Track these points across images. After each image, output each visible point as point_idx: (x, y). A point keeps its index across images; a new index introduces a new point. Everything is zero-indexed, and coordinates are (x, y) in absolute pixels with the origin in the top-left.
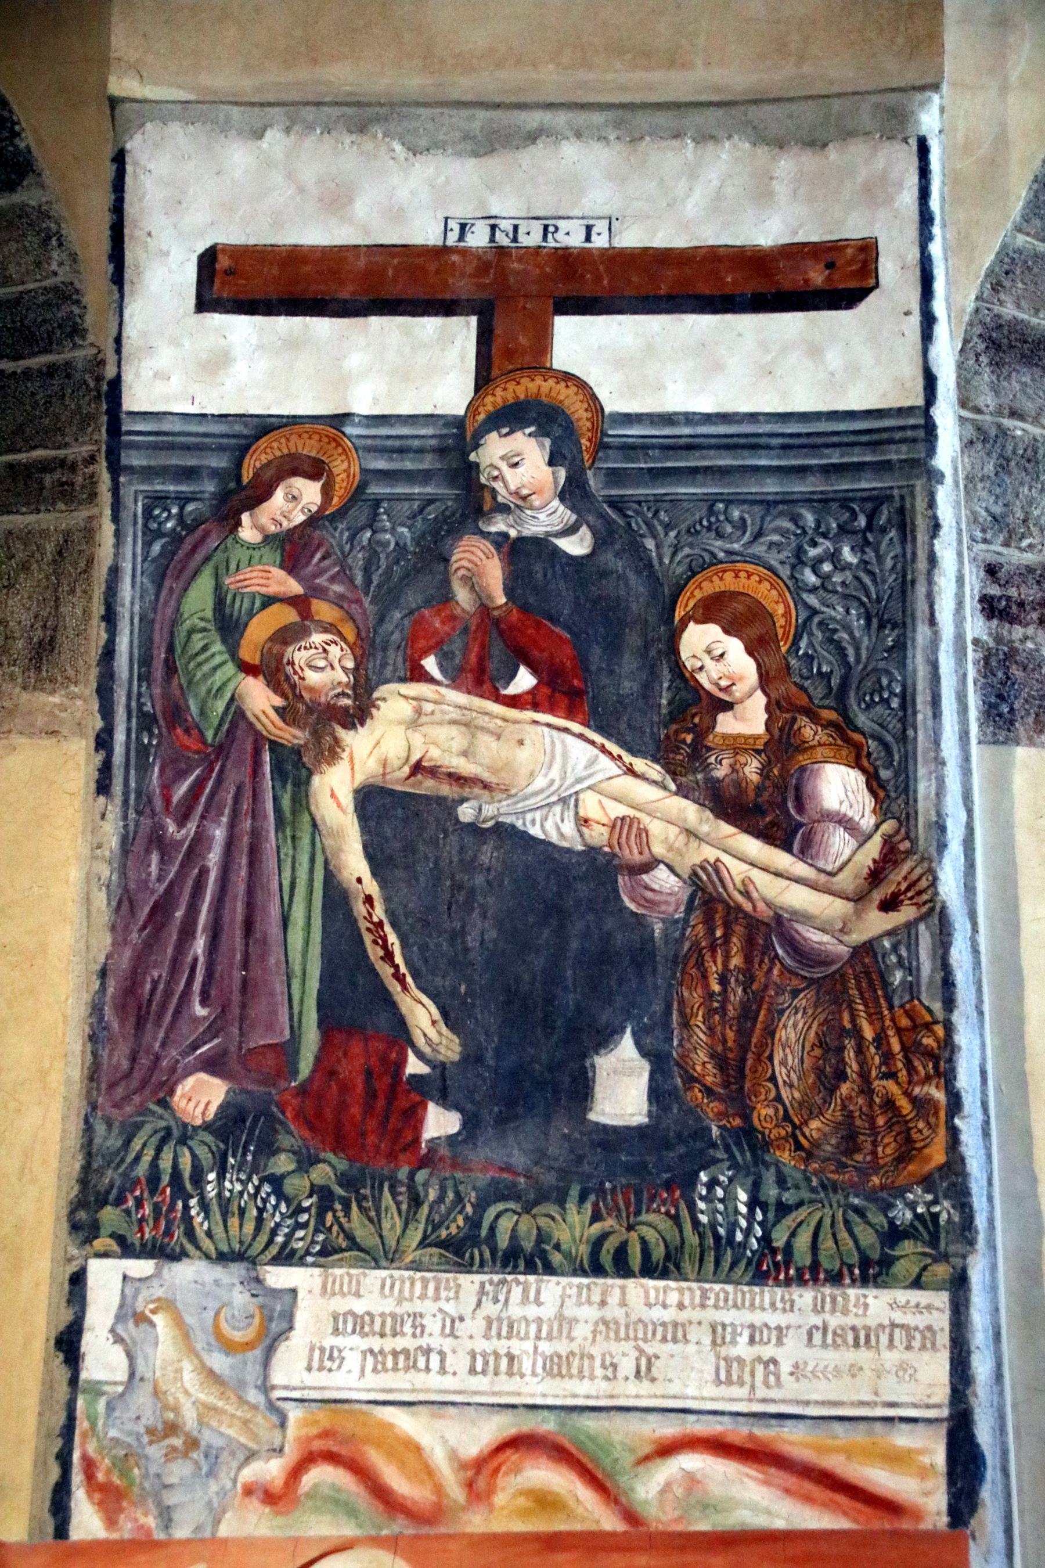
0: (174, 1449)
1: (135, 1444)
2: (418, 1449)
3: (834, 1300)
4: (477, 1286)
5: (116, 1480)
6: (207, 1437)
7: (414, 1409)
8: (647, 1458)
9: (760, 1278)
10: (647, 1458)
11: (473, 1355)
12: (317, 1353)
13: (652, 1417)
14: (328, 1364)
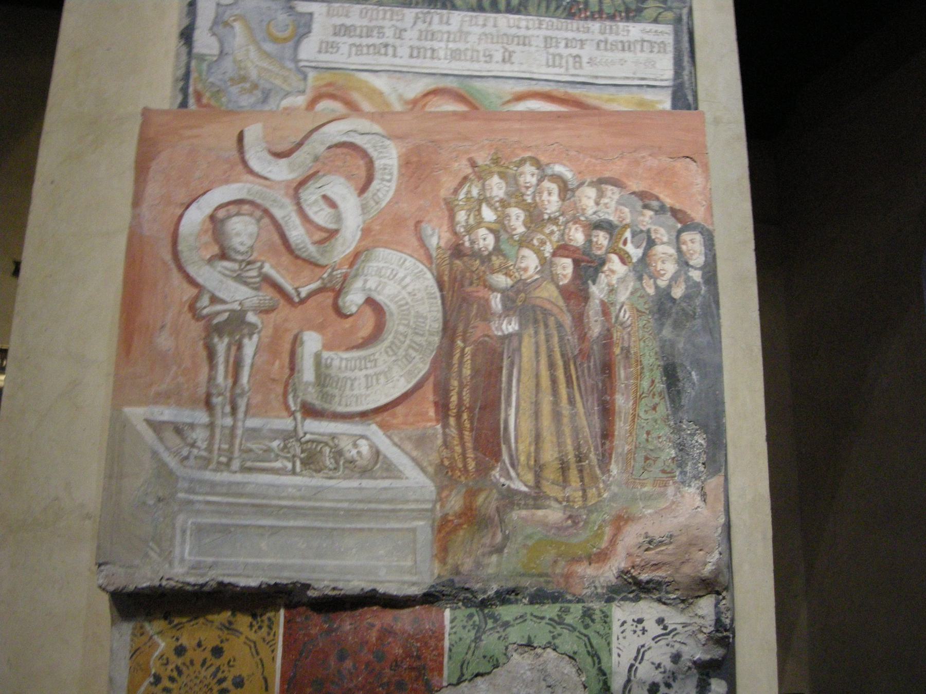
2: (381, 94)
3: (611, 27)
4: (413, 15)
5: (213, 102)
7: (379, 74)
8: (509, 102)
9: (571, 15)
10: (509, 102)
11: (412, 48)
12: (324, 45)
13: (511, 81)
14: (330, 50)
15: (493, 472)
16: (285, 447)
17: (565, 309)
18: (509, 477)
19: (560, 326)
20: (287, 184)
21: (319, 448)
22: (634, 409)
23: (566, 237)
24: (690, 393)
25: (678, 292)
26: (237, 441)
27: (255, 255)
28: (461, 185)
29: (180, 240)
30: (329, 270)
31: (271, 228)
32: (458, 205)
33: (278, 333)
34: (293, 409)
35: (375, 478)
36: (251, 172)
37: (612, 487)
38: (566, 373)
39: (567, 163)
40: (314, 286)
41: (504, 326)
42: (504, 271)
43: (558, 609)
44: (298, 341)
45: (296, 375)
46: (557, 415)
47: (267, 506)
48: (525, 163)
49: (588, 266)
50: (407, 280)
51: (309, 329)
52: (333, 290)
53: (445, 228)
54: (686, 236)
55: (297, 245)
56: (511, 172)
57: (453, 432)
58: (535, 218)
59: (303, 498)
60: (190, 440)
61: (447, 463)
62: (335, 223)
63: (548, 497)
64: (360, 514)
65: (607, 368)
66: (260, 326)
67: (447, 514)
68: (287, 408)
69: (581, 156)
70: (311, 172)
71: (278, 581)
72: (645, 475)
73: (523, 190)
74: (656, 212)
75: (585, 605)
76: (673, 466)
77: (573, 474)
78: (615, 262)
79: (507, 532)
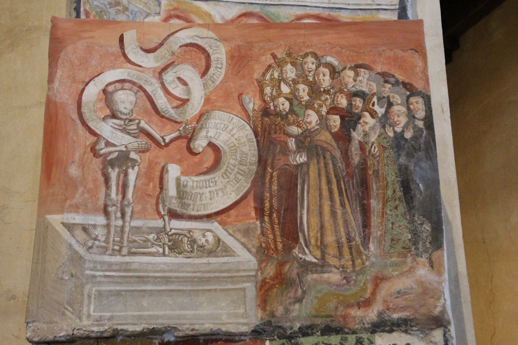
0: (119, 10)
1: (104, 8)
2: (210, 15)
6: (131, 7)
15: (294, 251)
16: (158, 238)
17: (336, 147)
18: (304, 253)
19: (333, 158)
20: (154, 70)
21: (180, 239)
22: (383, 209)
23: (335, 102)
24: (419, 198)
25: (408, 135)
26: (126, 236)
27: (134, 115)
28: (267, 70)
29: (83, 104)
30: (184, 125)
31: (145, 97)
32: (265, 83)
33: (151, 165)
34: (163, 213)
35: (218, 257)
36: (129, 61)
37: (371, 258)
38: (338, 187)
39: (335, 56)
40: (173, 135)
41: (297, 159)
42: (297, 124)
43: (340, 338)
44: (165, 170)
45: (164, 191)
46: (333, 213)
47: (147, 277)
48: (308, 55)
49: (350, 120)
50: (235, 131)
51: (171, 163)
52: (186, 137)
53: (258, 98)
54: (413, 100)
55: (162, 109)
56: (298, 61)
57: (267, 225)
58: (315, 90)
59: (171, 271)
60: (93, 236)
61: (264, 245)
62: (187, 95)
63: (330, 266)
64: (208, 280)
65: (364, 184)
66: (139, 161)
67: (266, 278)
68: (159, 213)
69: (344, 51)
70: (169, 62)
71: (155, 326)
72: (392, 250)
73: (307, 73)
74: (393, 85)
75: (358, 335)
76: (410, 244)
77: (346, 250)
78: (367, 117)
79: (305, 289)
